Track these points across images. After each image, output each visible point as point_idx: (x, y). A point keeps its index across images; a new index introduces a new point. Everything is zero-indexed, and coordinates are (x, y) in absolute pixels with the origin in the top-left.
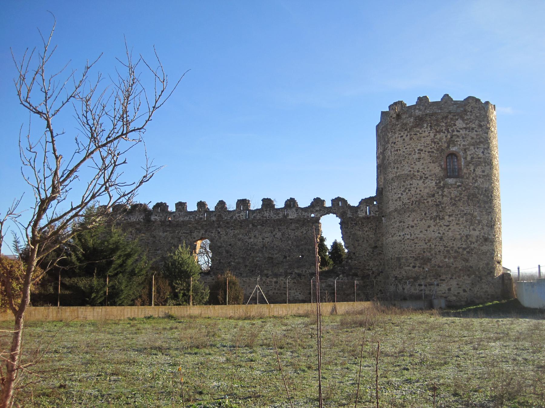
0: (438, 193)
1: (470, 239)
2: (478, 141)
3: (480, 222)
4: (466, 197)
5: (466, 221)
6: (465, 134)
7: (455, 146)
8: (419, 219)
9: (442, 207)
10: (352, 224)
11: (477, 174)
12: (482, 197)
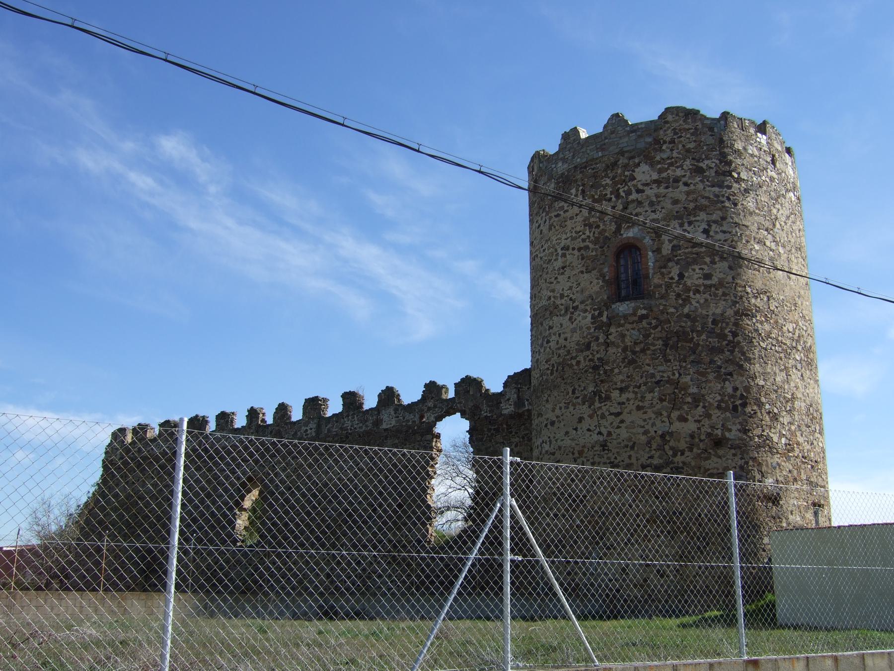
0: (597, 339)
1: (672, 443)
2: (691, 206)
3: (697, 400)
4: (660, 342)
5: (661, 400)
6: (657, 196)
7: (632, 226)
8: (562, 405)
9: (605, 372)
10: (489, 430)
11: (689, 283)
12: (704, 337)
